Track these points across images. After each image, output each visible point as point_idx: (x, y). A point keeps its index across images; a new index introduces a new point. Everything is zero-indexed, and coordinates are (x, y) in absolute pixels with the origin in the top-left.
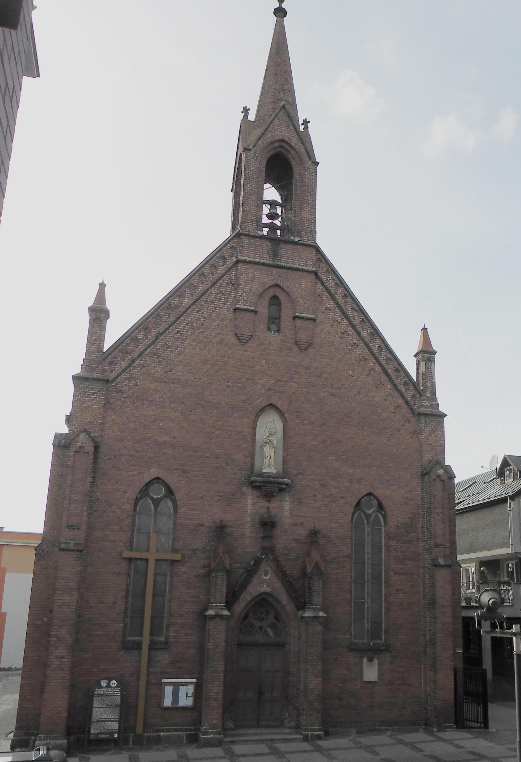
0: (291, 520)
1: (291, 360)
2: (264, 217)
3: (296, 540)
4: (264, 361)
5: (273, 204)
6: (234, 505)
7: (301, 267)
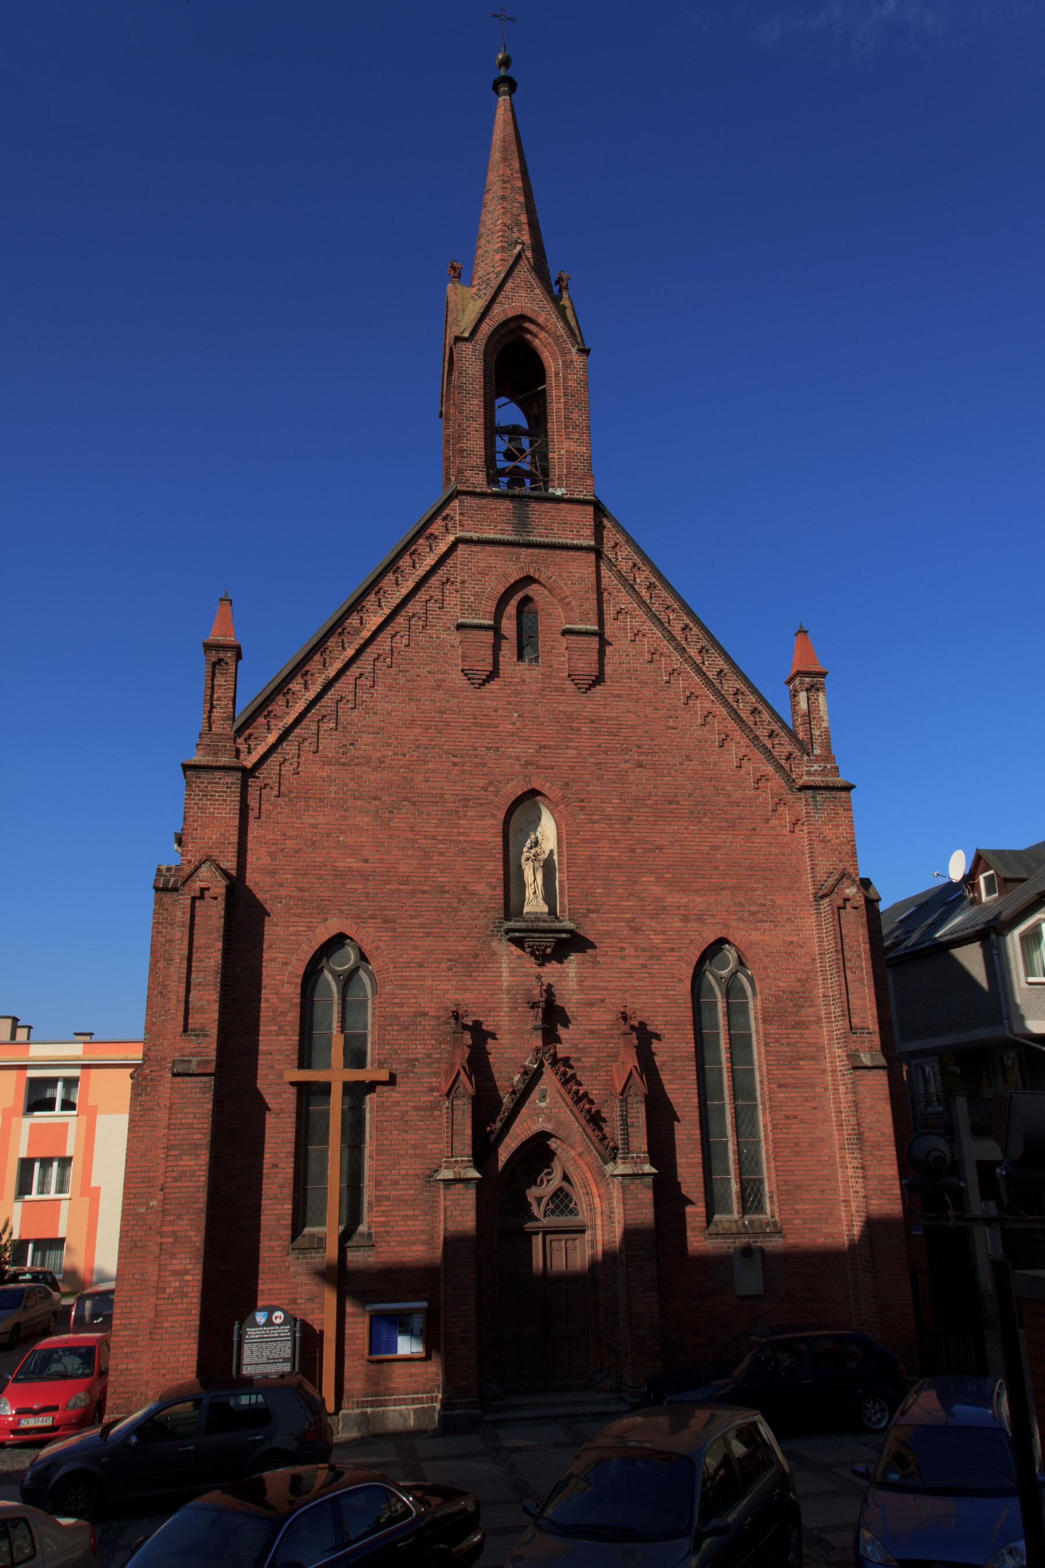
0: (580, 997)
1: (562, 708)
2: (500, 457)
3: (592, 1032)
4: (516, 715)
5: (514, 432)
6: (477, 974)
7: (569, 541)
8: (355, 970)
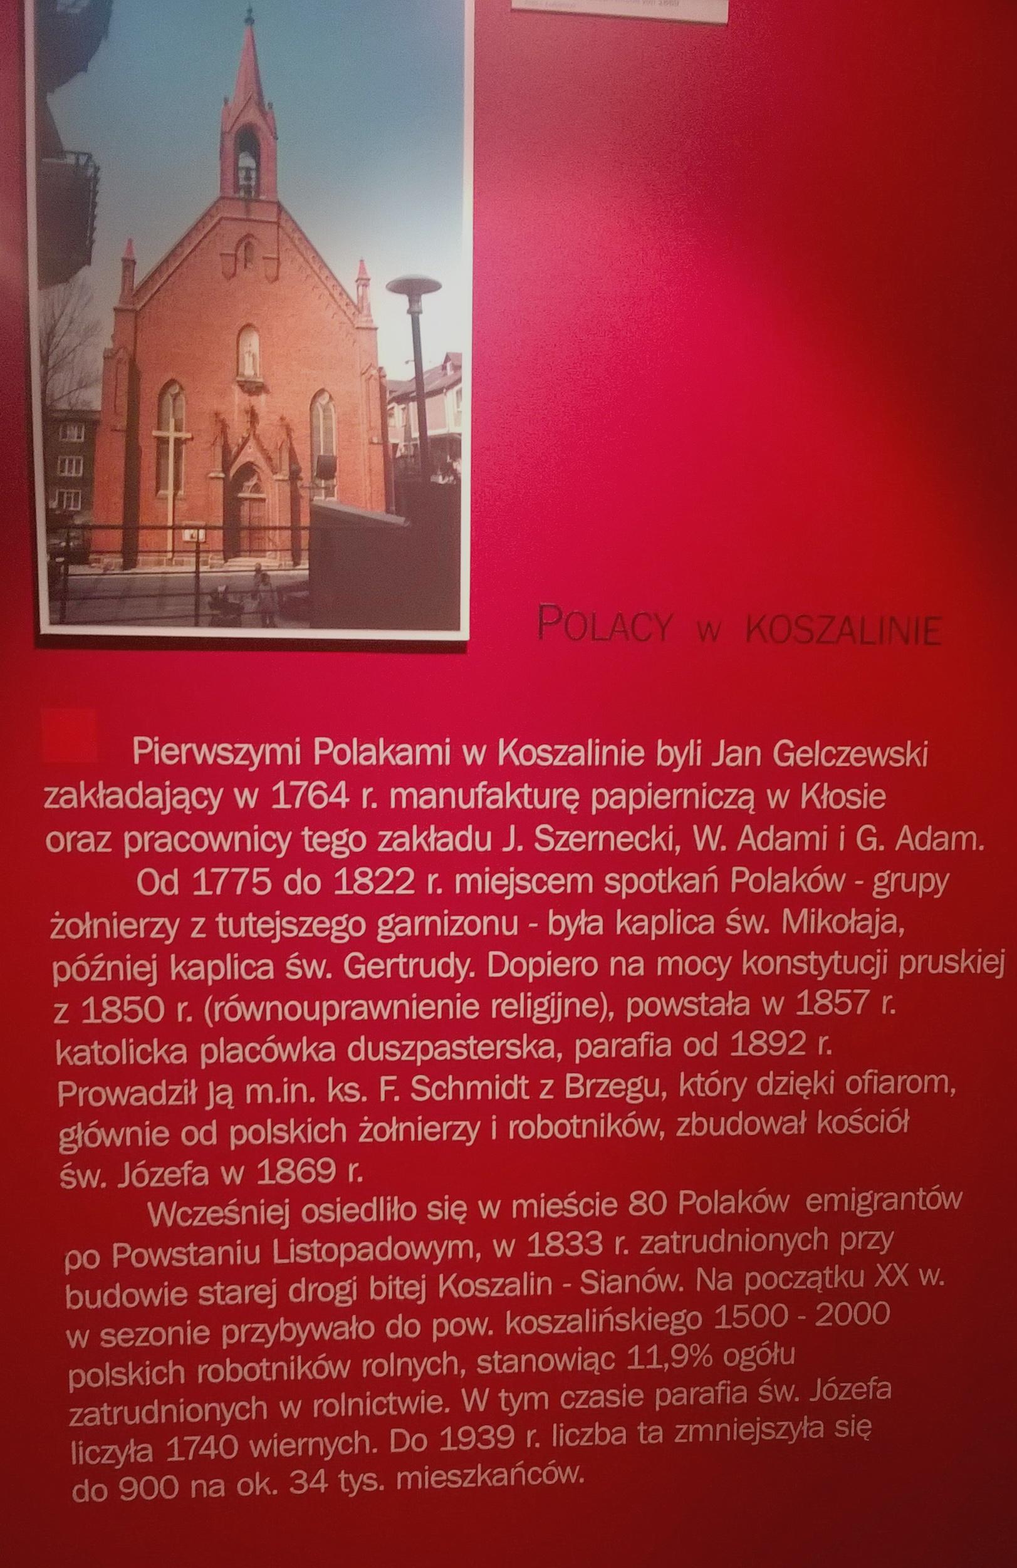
8: (178, 394)
